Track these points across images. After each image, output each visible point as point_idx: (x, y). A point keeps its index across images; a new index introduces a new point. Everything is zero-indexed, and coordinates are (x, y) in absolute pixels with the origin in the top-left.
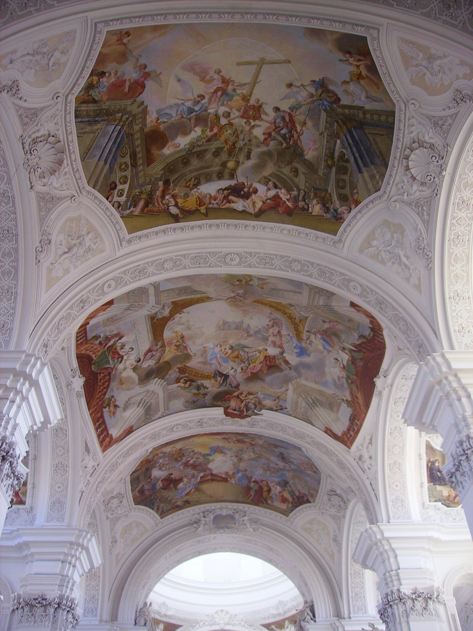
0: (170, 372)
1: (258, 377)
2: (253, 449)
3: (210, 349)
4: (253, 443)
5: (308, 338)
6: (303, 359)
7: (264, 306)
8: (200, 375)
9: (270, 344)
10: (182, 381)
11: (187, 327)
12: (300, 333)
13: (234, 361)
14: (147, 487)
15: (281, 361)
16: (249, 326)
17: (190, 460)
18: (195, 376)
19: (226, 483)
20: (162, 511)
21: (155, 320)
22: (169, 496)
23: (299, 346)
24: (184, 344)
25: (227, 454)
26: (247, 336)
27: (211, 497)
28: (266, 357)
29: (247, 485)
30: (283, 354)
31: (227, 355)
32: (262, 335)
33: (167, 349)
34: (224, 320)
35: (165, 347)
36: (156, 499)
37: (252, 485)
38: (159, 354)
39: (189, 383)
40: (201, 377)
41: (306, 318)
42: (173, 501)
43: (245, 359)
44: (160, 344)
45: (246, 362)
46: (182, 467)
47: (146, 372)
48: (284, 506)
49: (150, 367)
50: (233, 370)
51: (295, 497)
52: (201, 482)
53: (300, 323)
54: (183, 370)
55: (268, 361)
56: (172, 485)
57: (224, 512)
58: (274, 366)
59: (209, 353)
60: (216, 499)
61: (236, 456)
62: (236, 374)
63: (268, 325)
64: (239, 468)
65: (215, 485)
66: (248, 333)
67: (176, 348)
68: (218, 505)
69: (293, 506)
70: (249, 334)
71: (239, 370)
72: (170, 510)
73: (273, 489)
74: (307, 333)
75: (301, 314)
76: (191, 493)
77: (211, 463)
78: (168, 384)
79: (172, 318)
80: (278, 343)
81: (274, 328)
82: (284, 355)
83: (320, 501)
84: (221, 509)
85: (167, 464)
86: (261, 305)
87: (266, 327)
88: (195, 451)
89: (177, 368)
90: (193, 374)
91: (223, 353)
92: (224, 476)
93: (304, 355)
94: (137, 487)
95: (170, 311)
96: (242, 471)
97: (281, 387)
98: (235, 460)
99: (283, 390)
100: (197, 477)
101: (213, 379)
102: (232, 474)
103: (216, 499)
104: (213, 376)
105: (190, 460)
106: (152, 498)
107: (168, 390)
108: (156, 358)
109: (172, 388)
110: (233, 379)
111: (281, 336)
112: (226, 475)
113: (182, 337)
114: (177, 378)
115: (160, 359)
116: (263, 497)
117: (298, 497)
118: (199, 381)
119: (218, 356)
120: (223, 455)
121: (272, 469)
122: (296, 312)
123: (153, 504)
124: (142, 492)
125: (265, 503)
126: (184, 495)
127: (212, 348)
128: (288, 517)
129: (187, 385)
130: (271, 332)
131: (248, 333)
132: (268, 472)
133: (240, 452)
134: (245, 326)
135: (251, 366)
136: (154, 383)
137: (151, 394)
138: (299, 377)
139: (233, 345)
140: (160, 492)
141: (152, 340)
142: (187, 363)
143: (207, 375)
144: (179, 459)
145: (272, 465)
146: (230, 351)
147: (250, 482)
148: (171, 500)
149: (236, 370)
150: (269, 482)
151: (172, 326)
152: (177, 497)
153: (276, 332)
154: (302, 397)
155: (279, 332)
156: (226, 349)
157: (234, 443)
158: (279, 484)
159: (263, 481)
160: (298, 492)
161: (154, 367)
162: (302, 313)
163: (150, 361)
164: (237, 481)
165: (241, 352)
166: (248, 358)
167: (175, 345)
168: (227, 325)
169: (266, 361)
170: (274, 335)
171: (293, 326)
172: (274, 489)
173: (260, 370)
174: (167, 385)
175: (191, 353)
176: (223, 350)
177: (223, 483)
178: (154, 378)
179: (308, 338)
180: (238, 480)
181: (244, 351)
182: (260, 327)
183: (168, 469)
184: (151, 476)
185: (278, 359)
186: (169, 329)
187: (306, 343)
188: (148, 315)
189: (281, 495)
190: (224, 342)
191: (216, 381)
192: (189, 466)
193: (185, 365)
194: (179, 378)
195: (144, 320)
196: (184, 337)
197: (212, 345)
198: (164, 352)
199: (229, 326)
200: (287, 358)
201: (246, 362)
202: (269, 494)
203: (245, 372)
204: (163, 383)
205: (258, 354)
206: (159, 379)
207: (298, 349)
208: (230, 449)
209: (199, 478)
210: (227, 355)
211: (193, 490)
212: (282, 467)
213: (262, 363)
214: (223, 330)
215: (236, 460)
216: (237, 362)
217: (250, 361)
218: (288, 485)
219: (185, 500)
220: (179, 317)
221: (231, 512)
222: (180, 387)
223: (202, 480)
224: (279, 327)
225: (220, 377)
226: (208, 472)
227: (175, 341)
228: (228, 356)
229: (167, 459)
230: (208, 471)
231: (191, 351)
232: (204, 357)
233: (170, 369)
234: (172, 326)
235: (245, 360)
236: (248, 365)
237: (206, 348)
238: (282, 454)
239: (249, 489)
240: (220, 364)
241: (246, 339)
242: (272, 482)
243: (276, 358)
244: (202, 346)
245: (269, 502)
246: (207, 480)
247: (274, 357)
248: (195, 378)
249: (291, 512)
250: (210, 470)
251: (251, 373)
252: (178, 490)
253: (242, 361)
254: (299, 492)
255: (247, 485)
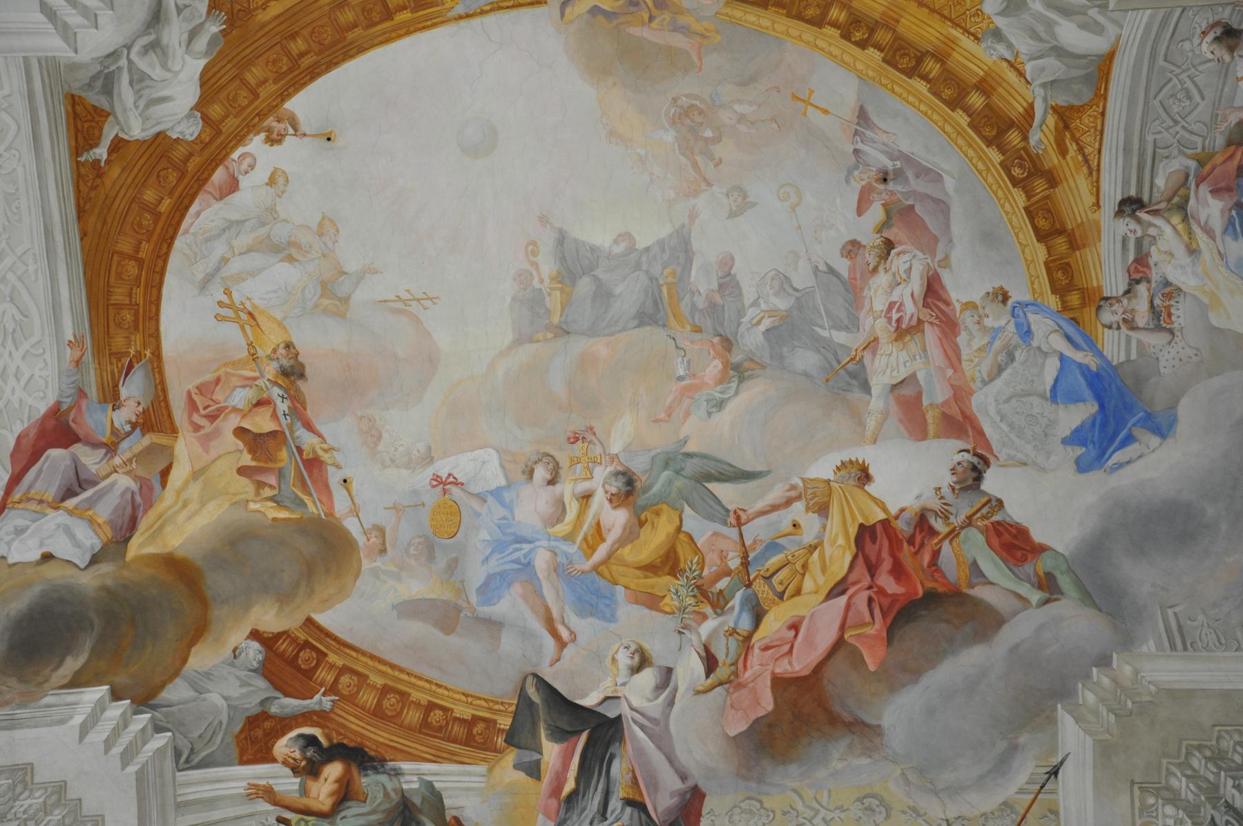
0: (201, 658)
1: (833, 720)
3: (482, 498)
5: (1139, 270)
6: (1124, 480)
7: (808, 32)
8: (412, 716)
9: (886, 415)
10: (284, 746)
11: (326, 288)
12: (1074, 245)
13: (652, 602)
15: (976, 546)
16: (728, 284)
18: (378, 713)
21: (101, 152)
23: (1085, 370)
24: (307, 440)
26: (723, 379)
28: (865, 534)
30: (979, 478)
31: (602, 551)
32: (823, 346)
33: (185, 449)
34: (562, 239)
35: (174, 431)
38: (124, 482)
39: (334, 770)
40: (425, 723)
41: (1105, 64)
43: (728, 573)
44: (134, 390)
45: (736, 601)
47: (19, 605)
49: (52, 572)
50: (648, 677)
53: (1063, 152)
54: (293, 662)
55: (887, 564)
58: (931, 598)
59: (480, 537)
62: (671, 703)
63: (852, 248)
66: (728, 344)
67: (247, 460)
70: (736, 358)
71: (690, 668)
74: (1125, 226)
75: (1059, 52)
78: (186, 759)
79: (219, 175)
80: (936, 394)
81: (898, 262)
82: (992, 483)
86: (796, 27)
87: (843, 266)
89: (255, 635)
90: (368, 698)
91: (569, 537)
93: (1129, 439)
95: (207, 80)
97: (1002, 765)
99: (1025, 771)
101: (511, 756)
104: (505, 722)
107: (182, 807)
108: (104, 512)
109: (206, 791)
110: (657, 758)
111: (949, 327)
113: (293, 373)
114: (253, 722)
115: (133, 524)
118: (405, 766)
119: (541, 560)
122: (1024, 45)
127: (497, 493)
129: (323, 790)
130: (880, 305)
131: (728, 344)
134: (702, 282)
135: (773, 624)
136: (78, 719)
137: (46, 809)
138: (1127, 642)
139: (638, 465)
141: (76, 343)
142: (327, 603)
143: (463, 711)
146: (617, 519)
149: (669, 671)
151: (220, 249)
153: (909, 293)
154: (1174, 799)
155: (933, 290)
156: (587, 497)
161: (88, 581)
162: (1070, 34)
163: (57, 518)
165: (693, 523)
166: (745, 564)
167: (240, 432)
168: (584, 286)
169: (872, 569)
170: (902, 332)
171: (1020, 198)
173: (839, 643)
174: (169, 763)
175: (351, 525)
176: (572, 509)
178: (76, 682)
179: (1139, 270)
181: (717, 511)
182: (802, 278)
185: (953, 534)
186: (200, 271)
187: (1130, 324)
188: (51, 67)
190: (574, 439)
191: (534, 770)
193: (309, 622)
194: (264, 716)
195: (20, 106)
196: (302, 376)
197: (492, 456)
198: (165, 474)
199: (603, 295)
200: (1016, 511)
201: (736, 601)
203: (733, 682)
204: (143, 736)
205: (811, 524)
206: (116, 695)
207: (1074, 398)
210: (602, 551)
213: (838, 589)
214: (563, 331)
216: (670, 602)
217: (760, 587)
220: (260, 175)
222: (268, 794)
224: (928, 242)
225: (559, 734)
227: (241, 397)
228: (605, 561)
231: (355, 512)
232: (442, 563)
233: (198, 631)
234: (220, 249)
235: (722, 584)
236: (745, 624)
237: (456, 491)
240: (554, 633)
241: (721, 405)
243: (939, 525)
244: (429, 472)
247: (922, 521)
248: (376, 736)
251: (780, 683)
253: (702, 592)
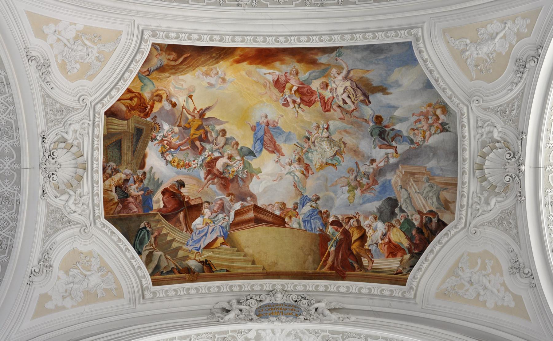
2: (327, 129)
4: (327, 94)
14: (134, 189)
17: (217, 159)
19: (281, 229)
20: (157, 267)
22: (174, 240)
25: (283, 155)
27: (253, 263)
29: (321, 230)
36: (148, 231)
37: (330, 230)
42: (181, 254)
46: (202, 173)
48: (394, 264)
51: (414, 232)
52: (235, 225)
56: (181, 215)
57: (279, 299)
60: (264, 269)
61: (300, 160)
64: (305, 194)
65: (261, 231)
68: (268, 284)
69: (412, 257)
72: (171, 271)
73: (369, 232)
76: (215, 246)
77: (255, 178)
83: (465, 202)
84: (272, 292)
85: (177, 148)
88: (228, 136)
92: (278, 213)
94: (115, 171)
96: (310, 200)
98: (298, 174)
100: (229, 212)
102: (291, 207)
103: (264, 269)
105: (217, 159)
106: (142, 225)
112: (281, 209)
116: (352, 253)
117: (420, 231)
120: (275, 156)
121: (364, 181)
123: (142, 243)
124: (121, 188)
125: (356, 266)
126: (203, 246)
128: (405, 285)
132: (358, 192)
133: (306, 145)
140: (159, 221)
144: (198, 143)
145: (362, 169)
147: (325, 225)
148: (178, 249)
150: (361, 219)
152: (190, 248)
157: (294, 102)
158: (380, 216)
159: (350, 218)
160: (418, 216)
164: (302, 223)
172: (371, 231)
177: (276, 228)
180: (304, 221)
183: (178, 166)
184: (142, 166)
189: (387, 240)
192: (216, 176)
202: (363, 246)
208: (288, 139)
209: (232, 214)
211: (221, 240)
212: (382, 164)
215: (297, 168)
218: (397, 210)
219: (202, 259)
221: (290, 301)
223: (238, 219)
226: (249, 202)
229: (176, 129)
230: (249, 199)
238: (378, 119)
239: (324, 239)
242: (366, 218)
245: (365, 261)
246: (248, 221)
249: (410, 271)
250: (253, 196)
252: (192, 231)
254: (420, 213)
255: (321, 230)
